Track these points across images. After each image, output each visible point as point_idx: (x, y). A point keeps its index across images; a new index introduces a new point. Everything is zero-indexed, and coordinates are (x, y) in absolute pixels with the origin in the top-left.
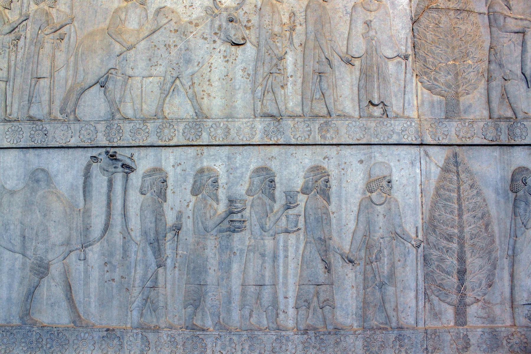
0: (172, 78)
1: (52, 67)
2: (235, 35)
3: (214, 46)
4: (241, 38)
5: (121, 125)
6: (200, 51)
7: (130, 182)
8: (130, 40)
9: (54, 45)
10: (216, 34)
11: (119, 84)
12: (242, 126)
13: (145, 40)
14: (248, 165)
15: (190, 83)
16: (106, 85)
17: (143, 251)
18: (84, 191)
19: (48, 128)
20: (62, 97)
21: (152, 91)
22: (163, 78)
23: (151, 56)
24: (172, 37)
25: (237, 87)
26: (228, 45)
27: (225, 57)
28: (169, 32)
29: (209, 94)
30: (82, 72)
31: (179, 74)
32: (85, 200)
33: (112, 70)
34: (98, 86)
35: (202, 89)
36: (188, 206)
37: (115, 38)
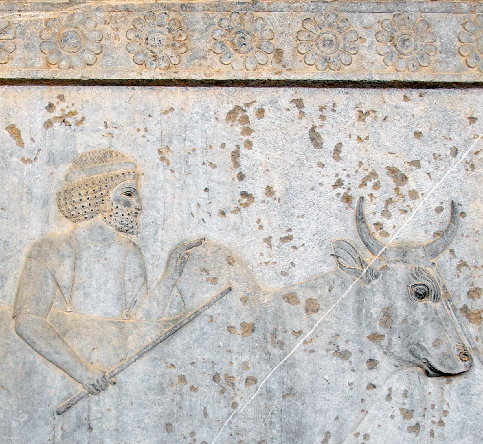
2: (437, 343)
3: (372, 376)
6: (328, 396)
8: (95, 356)
10: (375, 337)
13: (145, 358)
24: (235, 348)
28: (226, 333)
37: (44, 350)
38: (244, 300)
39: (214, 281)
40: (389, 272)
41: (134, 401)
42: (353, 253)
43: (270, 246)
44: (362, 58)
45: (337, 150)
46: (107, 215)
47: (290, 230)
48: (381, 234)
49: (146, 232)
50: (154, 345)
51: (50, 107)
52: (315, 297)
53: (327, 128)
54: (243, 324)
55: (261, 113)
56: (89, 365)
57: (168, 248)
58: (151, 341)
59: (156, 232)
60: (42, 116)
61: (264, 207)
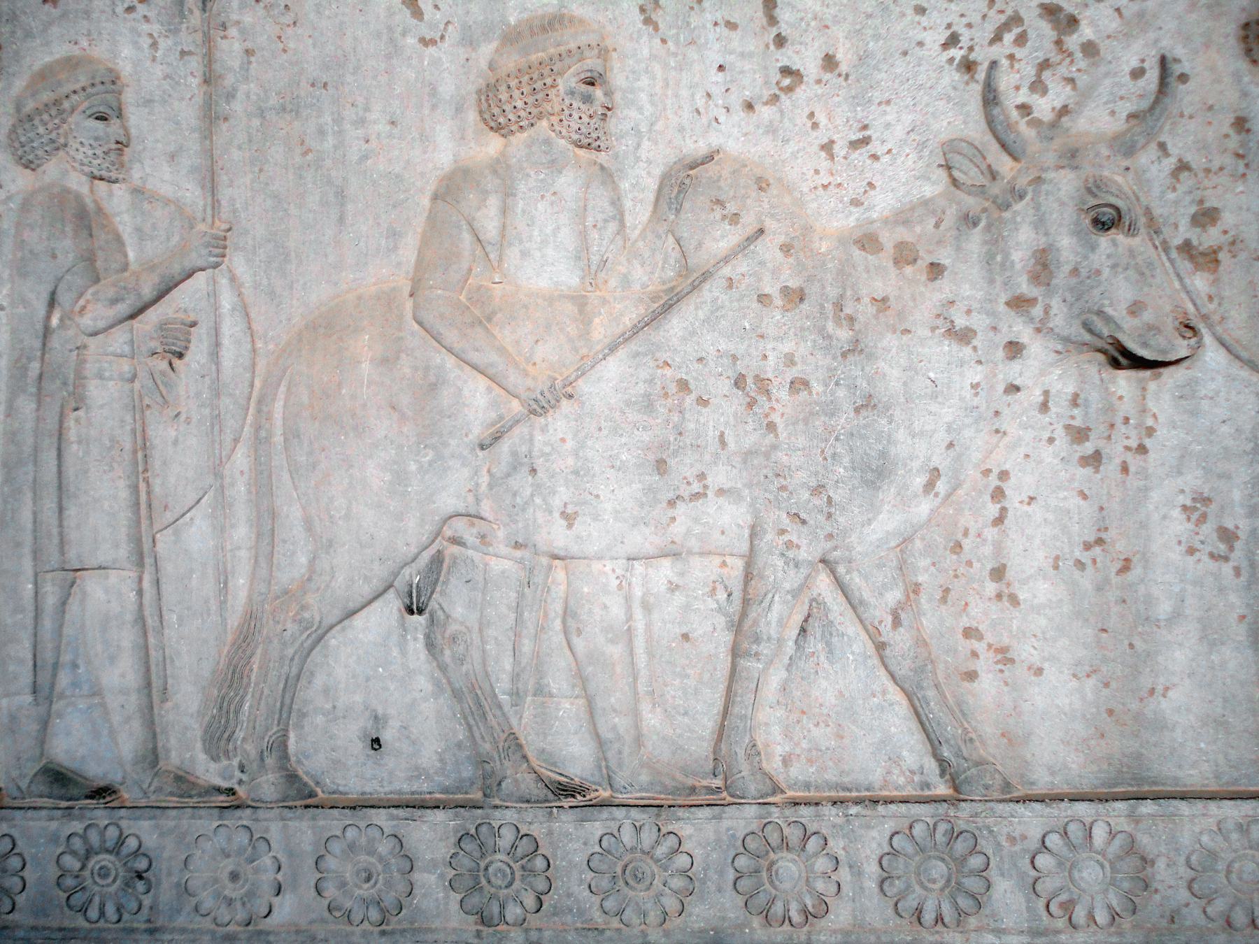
0: (792, 572)
2: (1135, 308)
4: (1170, 325)
5: (537, 830)
6: (934, 407)
8: (541, 352)
9: (137, 385)
10: (1019, 303)
11: (504, 599)
13: (622, 353)
15: (894, 596)
16: (433, 605)
19: (151, 841)
20: (206, 670)
21: (686, 637)
23: (663, 446)
24: (771, 331)
25: (1164, 608)
26: (1094, 367)
27: (1079, 435)
28: (755, 305)
29: (1003, 650)
30: (298, 532)
31: (829, 545)
34: (392, 605)
35: (965, 622)
37: (457, 347)
38: (786, 249)
39: (735, 219)
40: (1045, 187)
41: (603, 424)
42: (978, 160)
43: (832, 157)
46: (555, 120)
47: (865, 127)
48: (1029, 123)
49: (624, 146)
50: (636, 330)
52: (910, 239)
54: (785, 291)
56: (530, 368)
57: (658, 171)
58: (629, 324)
59: (639, 145)
61: (819, 90)
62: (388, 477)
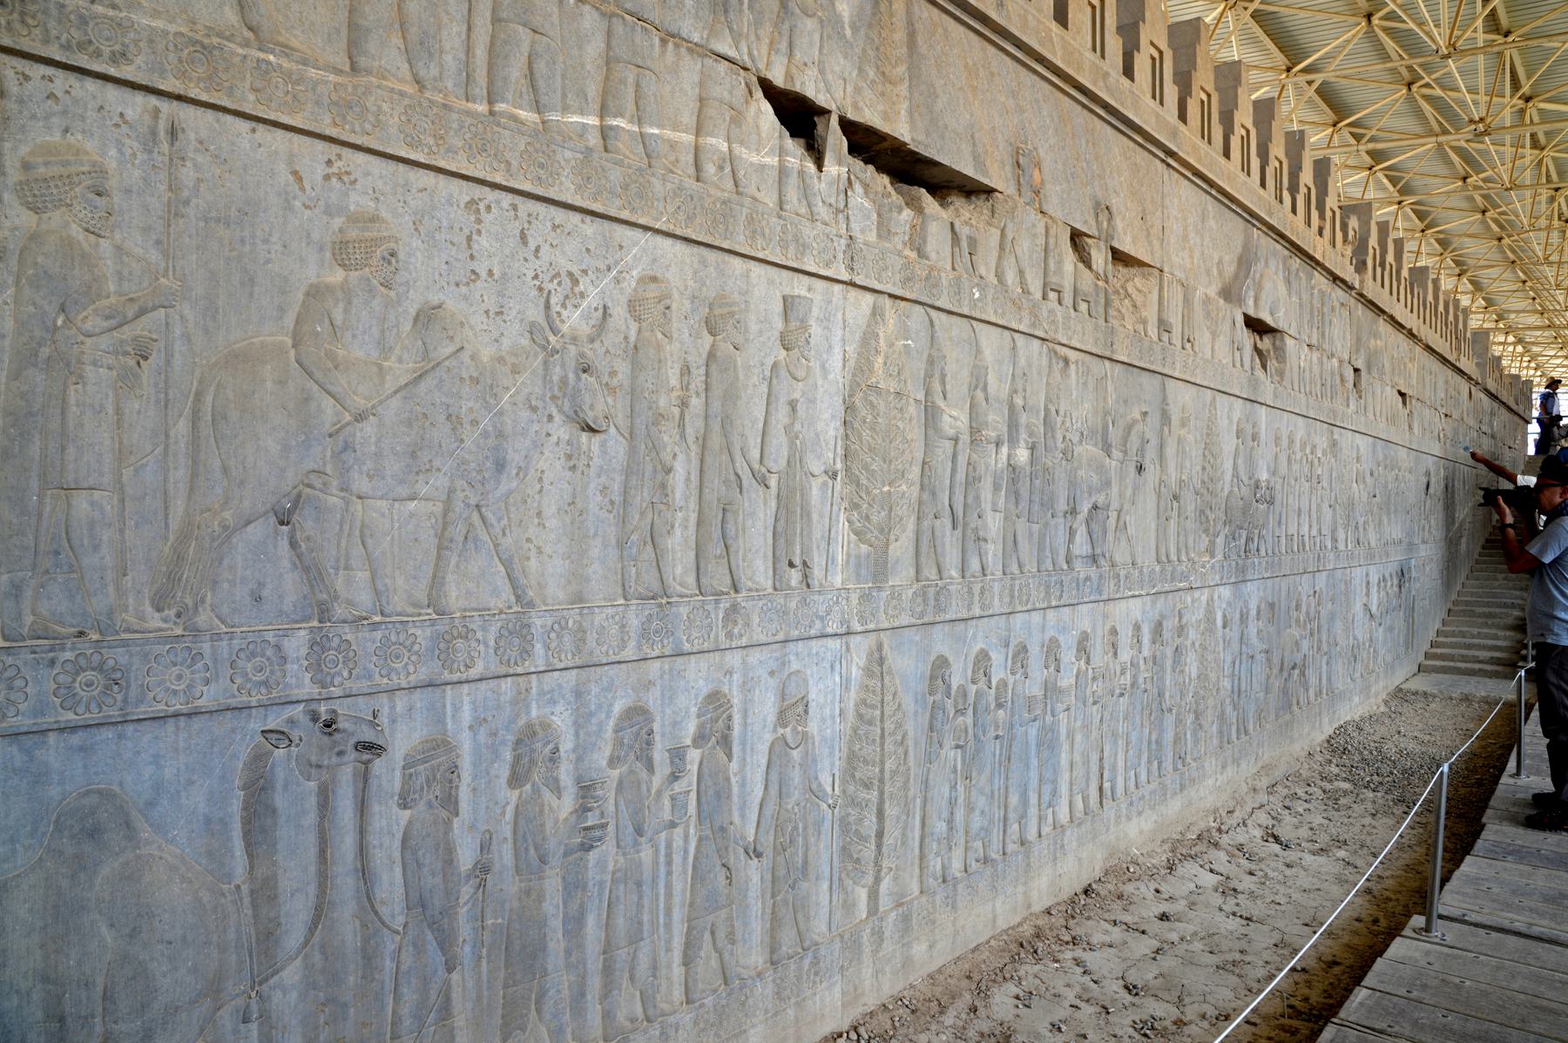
1: (121, 454)
5: (349, 637)
7: (373, 783)
10: (553, 398)
12: (606, 624)
13: (398, 396)
14: (611, 705)
17: (415, 945)
18: (247, 834)
19: (123, 660)
22: (440, 505)
25: (592, 532)
27: (569, 457)
29: (539, 548)
32: (250, 855)
33: (312, 476)
36: (504, 813)
44: (561, 183)
45: (537, 250)
50: (406, 385)
51: (329, 162)
53: (532, 232)
55: (489, 208)
60: (321, 170)
62: (279, 447)
